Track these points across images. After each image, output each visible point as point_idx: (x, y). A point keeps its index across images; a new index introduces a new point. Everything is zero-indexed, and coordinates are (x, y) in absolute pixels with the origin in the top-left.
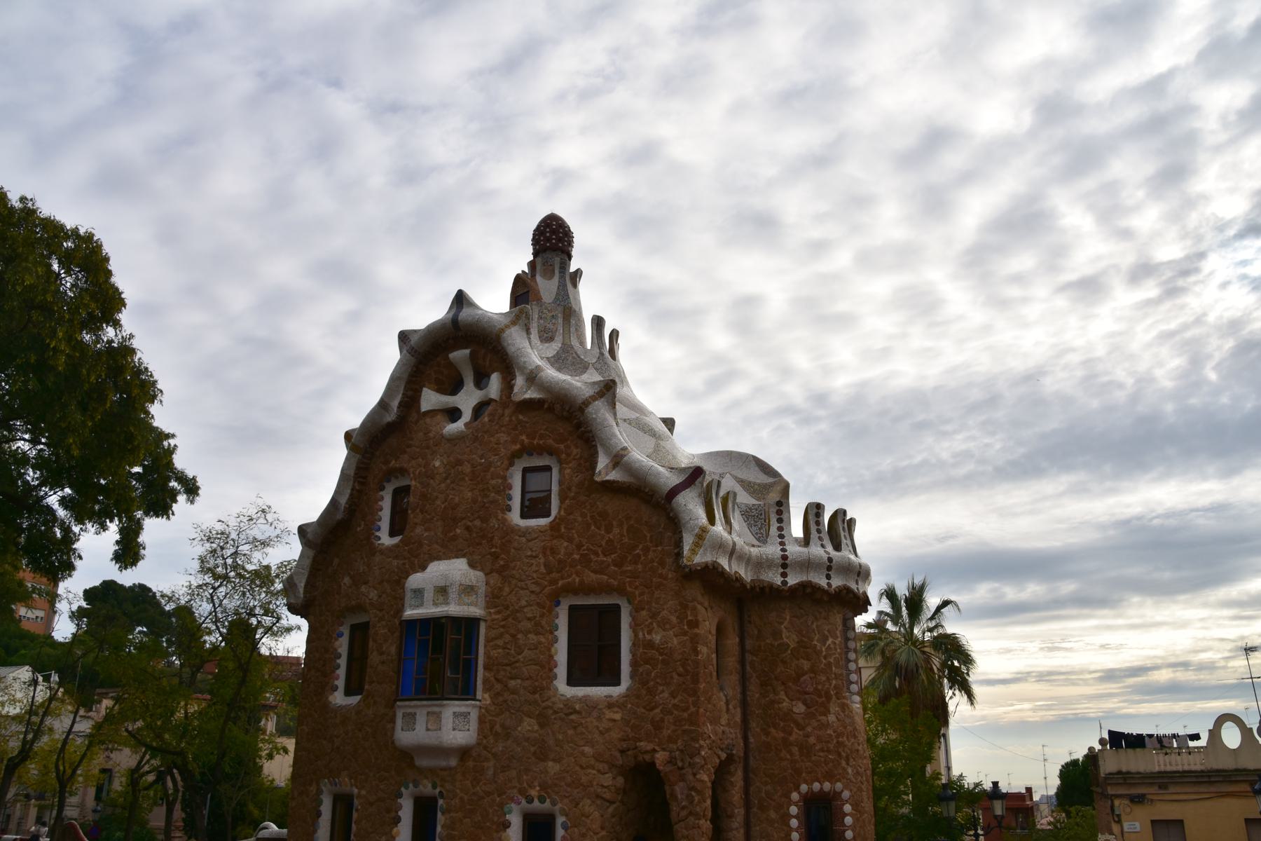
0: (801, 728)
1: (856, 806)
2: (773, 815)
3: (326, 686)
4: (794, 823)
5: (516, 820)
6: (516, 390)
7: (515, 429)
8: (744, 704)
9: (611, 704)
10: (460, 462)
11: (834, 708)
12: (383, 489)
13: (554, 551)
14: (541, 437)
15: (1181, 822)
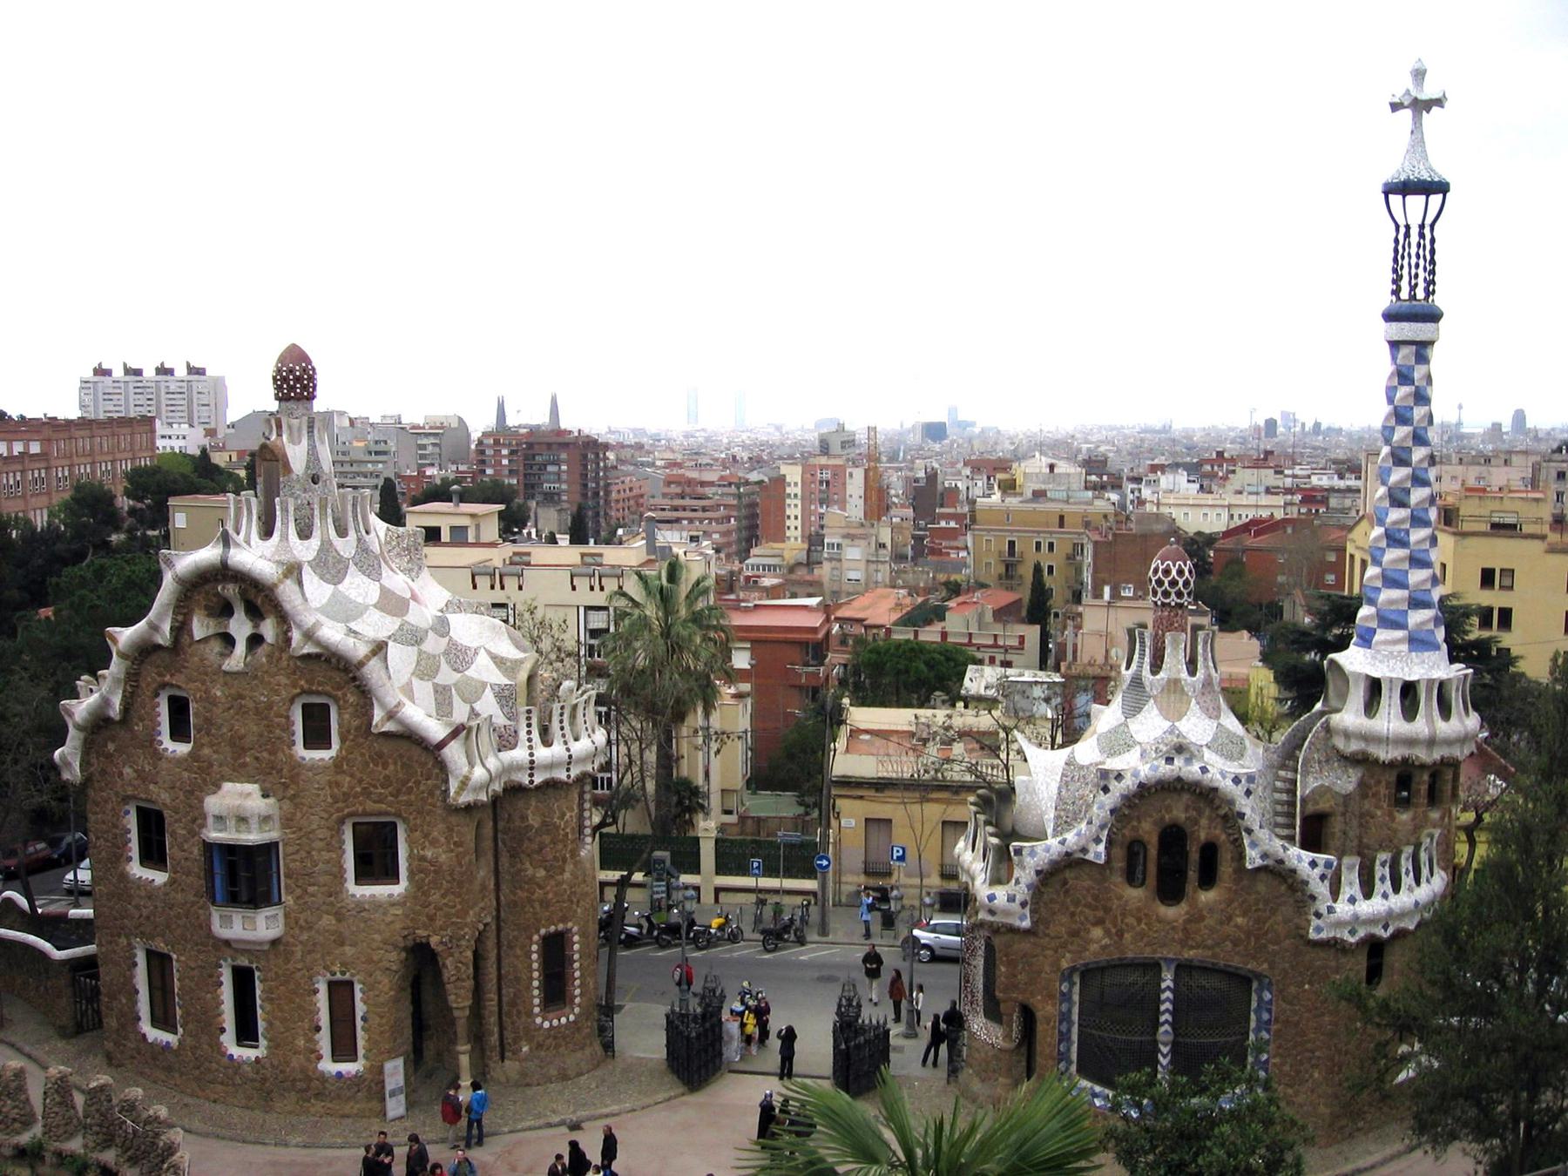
0: (541, 887)
1: (583, 934)
2: (519, 952)
3: (119, 857)
4: (535, 956)
5: (323, 988)
6: (294, 644)
7: (294, 673)
8: (497, 872)
9: (393, 903)
10: (241, 697)
11: (569, 867)
12: (157, 695)
13: (338, 784)
14: (319, 684)
15: (890, 821)
